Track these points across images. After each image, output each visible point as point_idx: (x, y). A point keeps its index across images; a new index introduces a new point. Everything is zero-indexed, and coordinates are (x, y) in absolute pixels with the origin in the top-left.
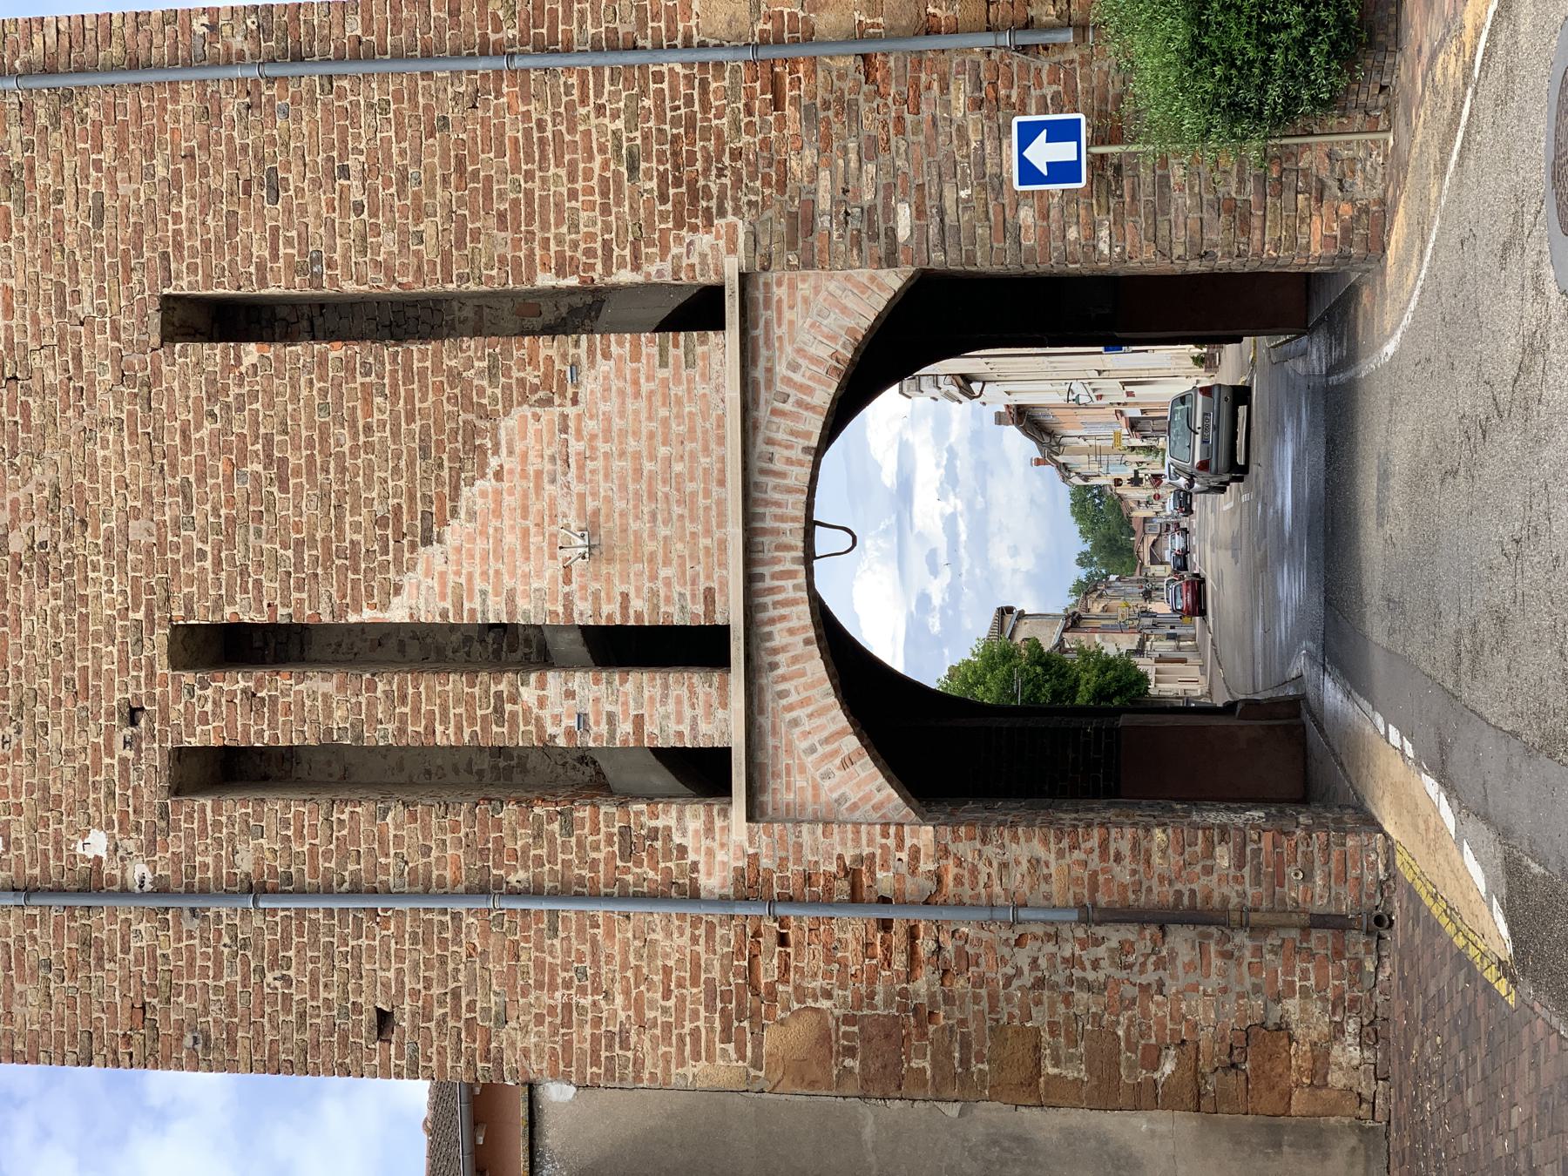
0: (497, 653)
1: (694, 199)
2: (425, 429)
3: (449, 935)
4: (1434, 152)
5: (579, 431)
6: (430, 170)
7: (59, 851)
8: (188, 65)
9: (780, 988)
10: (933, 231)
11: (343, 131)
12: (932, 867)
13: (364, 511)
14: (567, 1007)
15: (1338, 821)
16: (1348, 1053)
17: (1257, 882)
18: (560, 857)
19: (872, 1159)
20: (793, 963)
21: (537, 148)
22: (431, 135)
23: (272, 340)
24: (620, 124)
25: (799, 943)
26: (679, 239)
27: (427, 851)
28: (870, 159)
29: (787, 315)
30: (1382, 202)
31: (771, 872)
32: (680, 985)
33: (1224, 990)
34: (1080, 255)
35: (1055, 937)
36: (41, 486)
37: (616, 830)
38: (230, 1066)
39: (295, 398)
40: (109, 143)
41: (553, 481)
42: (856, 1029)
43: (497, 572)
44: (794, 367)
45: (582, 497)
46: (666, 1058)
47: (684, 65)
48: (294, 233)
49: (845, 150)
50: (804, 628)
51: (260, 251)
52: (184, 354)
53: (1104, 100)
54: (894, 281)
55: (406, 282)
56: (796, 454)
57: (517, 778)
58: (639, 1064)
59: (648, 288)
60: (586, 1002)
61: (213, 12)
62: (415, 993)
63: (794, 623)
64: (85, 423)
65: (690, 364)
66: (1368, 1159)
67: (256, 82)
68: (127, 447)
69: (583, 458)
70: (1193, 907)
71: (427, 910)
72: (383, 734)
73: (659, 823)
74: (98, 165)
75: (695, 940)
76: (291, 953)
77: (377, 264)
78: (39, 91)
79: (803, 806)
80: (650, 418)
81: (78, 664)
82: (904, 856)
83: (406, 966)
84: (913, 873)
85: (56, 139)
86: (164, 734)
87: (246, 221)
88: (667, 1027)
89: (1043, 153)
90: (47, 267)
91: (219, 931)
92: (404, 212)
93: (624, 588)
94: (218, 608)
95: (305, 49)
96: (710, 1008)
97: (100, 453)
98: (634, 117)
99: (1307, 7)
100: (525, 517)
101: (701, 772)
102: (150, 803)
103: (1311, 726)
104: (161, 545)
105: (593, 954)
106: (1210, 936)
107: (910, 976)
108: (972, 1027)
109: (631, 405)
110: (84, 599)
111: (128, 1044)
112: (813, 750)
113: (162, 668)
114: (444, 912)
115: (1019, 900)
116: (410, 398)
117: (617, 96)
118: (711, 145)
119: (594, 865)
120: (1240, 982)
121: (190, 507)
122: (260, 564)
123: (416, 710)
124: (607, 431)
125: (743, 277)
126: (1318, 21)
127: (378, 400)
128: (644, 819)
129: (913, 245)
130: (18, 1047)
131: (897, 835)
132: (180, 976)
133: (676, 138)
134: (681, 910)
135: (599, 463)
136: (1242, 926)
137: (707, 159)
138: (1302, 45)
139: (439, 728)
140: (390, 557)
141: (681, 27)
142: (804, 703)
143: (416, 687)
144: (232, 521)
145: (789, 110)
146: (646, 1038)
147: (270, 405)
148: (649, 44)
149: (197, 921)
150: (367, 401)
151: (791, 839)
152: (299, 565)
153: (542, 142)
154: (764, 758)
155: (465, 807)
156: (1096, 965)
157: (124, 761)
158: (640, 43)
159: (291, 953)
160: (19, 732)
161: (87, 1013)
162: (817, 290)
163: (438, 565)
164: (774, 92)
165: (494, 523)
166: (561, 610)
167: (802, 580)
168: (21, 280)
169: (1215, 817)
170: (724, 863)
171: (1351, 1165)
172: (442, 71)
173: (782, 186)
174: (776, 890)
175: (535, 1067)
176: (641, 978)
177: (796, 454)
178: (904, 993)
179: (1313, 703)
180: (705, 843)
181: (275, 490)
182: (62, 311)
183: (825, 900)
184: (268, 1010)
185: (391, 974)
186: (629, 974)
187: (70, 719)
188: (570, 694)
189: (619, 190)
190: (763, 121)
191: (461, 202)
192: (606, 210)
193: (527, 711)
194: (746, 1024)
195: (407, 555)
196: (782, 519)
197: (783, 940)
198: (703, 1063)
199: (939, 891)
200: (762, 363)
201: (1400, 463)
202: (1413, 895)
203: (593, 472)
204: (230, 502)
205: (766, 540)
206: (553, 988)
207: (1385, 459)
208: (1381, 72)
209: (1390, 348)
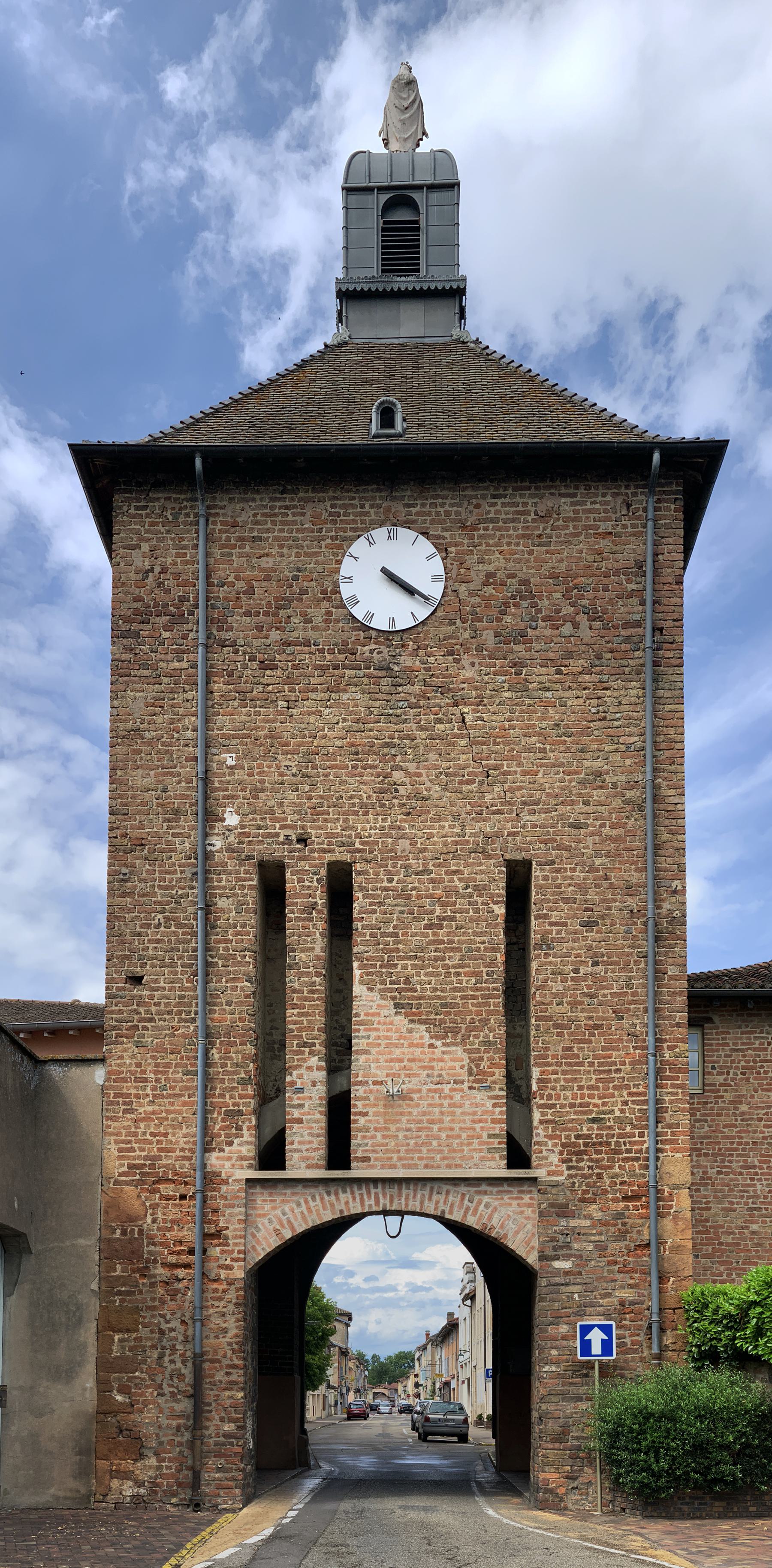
0: (335, 1044)
1: (577, 1153)
2: (457, 1005)
3: (184, 1016)
4: (592, 1535)
5: (455, 1090)
6: (595, 1010)
8: (655, 877)
9: (157, 1196)
10: (557, 1280)
11: (617, 963)
12: (222, 1277)
13: (414, 971)
14: (145, 1080)
15: (248, 1485)
16: (129, 1490)
17: (217, 1444)
19: (68, 1243)
20: (171, 1202)
21: (606, 1069)
22: (614, 1012)
23: (507, 921)
24: (617, 1114)
25: (181, 1206)
26: (555, 1145)
27: (229, 1004)
28: (595, 1247)
29: (515, 1203)
30: (566, 1509)
31: (219, 1191)
32: (158, 1142)
33: (160, 1427)
34: (543, 1356)
35: (186, 1341)
36: (428, 790)
38: (111, 893)
39: (475, 934)
40: (614, 832)
41: (428, 1076)
43: (380, 1045)
44: (487, 1206)
45: (420, 1091)
46: (119, 1134)
47: (647, 1149)
48: (564, 935)
49: (600, 1234)
50: (349, 1210)
51: (555, 916)
52: (500, 872)
53: (622, 1369)
54: (532, 1259)
55: (536, 997)
56: (441, 1206)
57: (269, 1054)
58: (116, 1119)
59: (530, 1128)
60: (148, 1091)
61: (683, 892)
63: (351, 1205)
64: (464, 816)
66: (74, 1499)
67: (645, 915)
68: (450, 839)
69: (440, 1092)
70: (203, 1412)
71: (197, 1004)
72: (293, 981)
73: (245, 1132)
74: (603, 826)
75: (182, 1150)
76: (173, 929)
77: (546, 981)
78: (644, 793)
79: (255, 1208)
80: (461, 1128)
81: (331, 810)
82: (228, 1262)
83: (167, 992)
84: (219, 1267)
86: (289, 858)
88: (135, 1135)
89: (596, 1337)
90: (549, 795)
91: (184, 888)
92: (574, 996)
93: (371, 1113)
94: (362, 889)
95: (662, 943)
96: (146, 1158)
97: (446, 824)
98: (620, 1121)
99: (667, 1472)
100: (409, 1060)
101: (272, 1154)
102: (254, 850)
103: (295, 1472)
104: (396, 858)
105: (174, 1095)
106: (188, 1420)
107: (164, 1265)
108: (139, 1297)
109: (467, 1118)
110: (366, 813)
111: (122, 836)
112: (284, 1214)
113: (328, 857)
114: (196, 1013)
115: (205, 1322)
116: (474, 997)
117: (633, 1111)
118: (605, 1163)
120: (165, 1435)
121: (417, 874)
122: (385, 913)
123: (306, 999)
124: (454, 1105)
125: (535, 1179)
126: (659, 1477)
127: (473, 980)
128: (247, 1123)
129: (550, 1269)
130: (119, 773)
132: (160, 866)
133: (609, 1144)
134: (198, 1143)
135: (437, 1101)
136: (194, 1436)
137: (598, 1161)
138: (648, 1469)
139: (295, 1011)
140: (388, 986)
141: (668, 1147)
142: (309, 1209)
143: (318, 999)
144: (409, 897)
145: (622, 1204)
146: (129, 1123)
147: (472, 920)
148: (659, 1130)
150: (473, 974)
151: (236, 1202)
152: (384, 935)
154: (280, 1189)
155: (253, 1025)
156: (172, 1361)
157: (277, 835)
158: (660, 1125)
159: (173, 929)
160: (293, 775)
161: (139, 813)
162: (527, 1218)
164: (632, 1196)
165: (406, 1043)
166: (359, 1079)
167: (374, 1209)
168: (541, 781)
169: (249, 1423)
170: (223, 1166)
171: (71, 1490)
172: (648, 1018)
174: (209, 1194)
175: (113, 1062)
176: (161, 1120)
177: (441, 1206)
178: (155, 1261)
179: (307, 1474)
180: (235, 1156)
181: (426, 922)
182: (525, 803)
183: (204, 1221)
184: (142, 915)
185: (162, 984)
186: (164, 1114)
187: (300, 805)
188: (314, 1084)
190: (617, 1191)
194: (138, 1177)
196: (407, 1199)
197: (183, 1197)
198: (117, 1154)
199: (210, 1280)
200: (489, 1189)
201: (432, 1518)
202: (211, 1522)
203: (433, 1097)
205: (396, 1190)
206: (156, 1072)
207: (433, 1510)
208: (632, 1509)
209: (491, 1512)
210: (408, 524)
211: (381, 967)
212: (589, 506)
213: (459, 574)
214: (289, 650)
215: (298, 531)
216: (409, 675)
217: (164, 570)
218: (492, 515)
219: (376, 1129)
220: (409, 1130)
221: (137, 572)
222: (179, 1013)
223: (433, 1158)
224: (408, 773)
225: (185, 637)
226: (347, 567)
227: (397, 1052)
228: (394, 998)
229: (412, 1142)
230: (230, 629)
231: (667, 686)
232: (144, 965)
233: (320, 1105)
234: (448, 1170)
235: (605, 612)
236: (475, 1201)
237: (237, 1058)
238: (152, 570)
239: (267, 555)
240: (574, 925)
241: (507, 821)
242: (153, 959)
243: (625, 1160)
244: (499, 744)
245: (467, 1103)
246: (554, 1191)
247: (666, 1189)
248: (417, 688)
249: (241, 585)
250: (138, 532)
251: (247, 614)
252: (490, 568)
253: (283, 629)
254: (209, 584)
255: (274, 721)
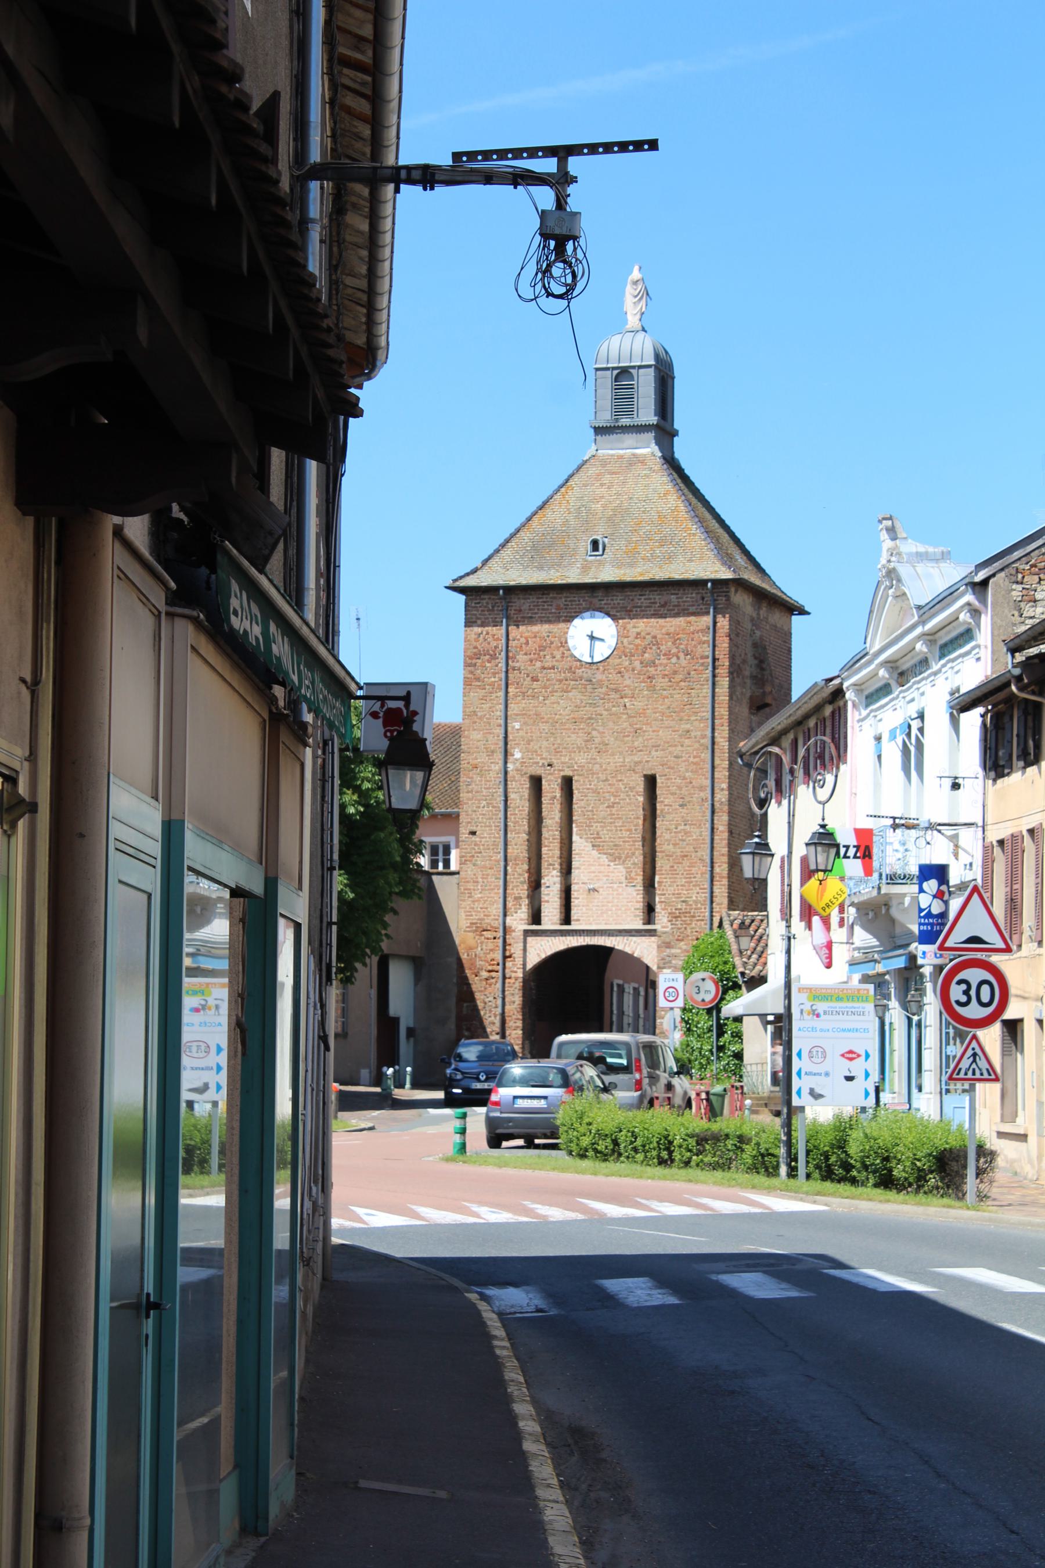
51: (667, 801)
65: (636, 916)
72: (545, 834)
98: (696, 902)
101: (536, 917)
113: (562, 774)
125: (655, 930)
176: (485, 901)
183: (504, 950)
210: (600, 610)
216: (600, 684)
224: (599, 732)
227: (593, 868)
237: (519, 871)
248: (604, 689)
249: (523, 640)
251: (526, 654)
252: (638, 630)
254: (508, 639)
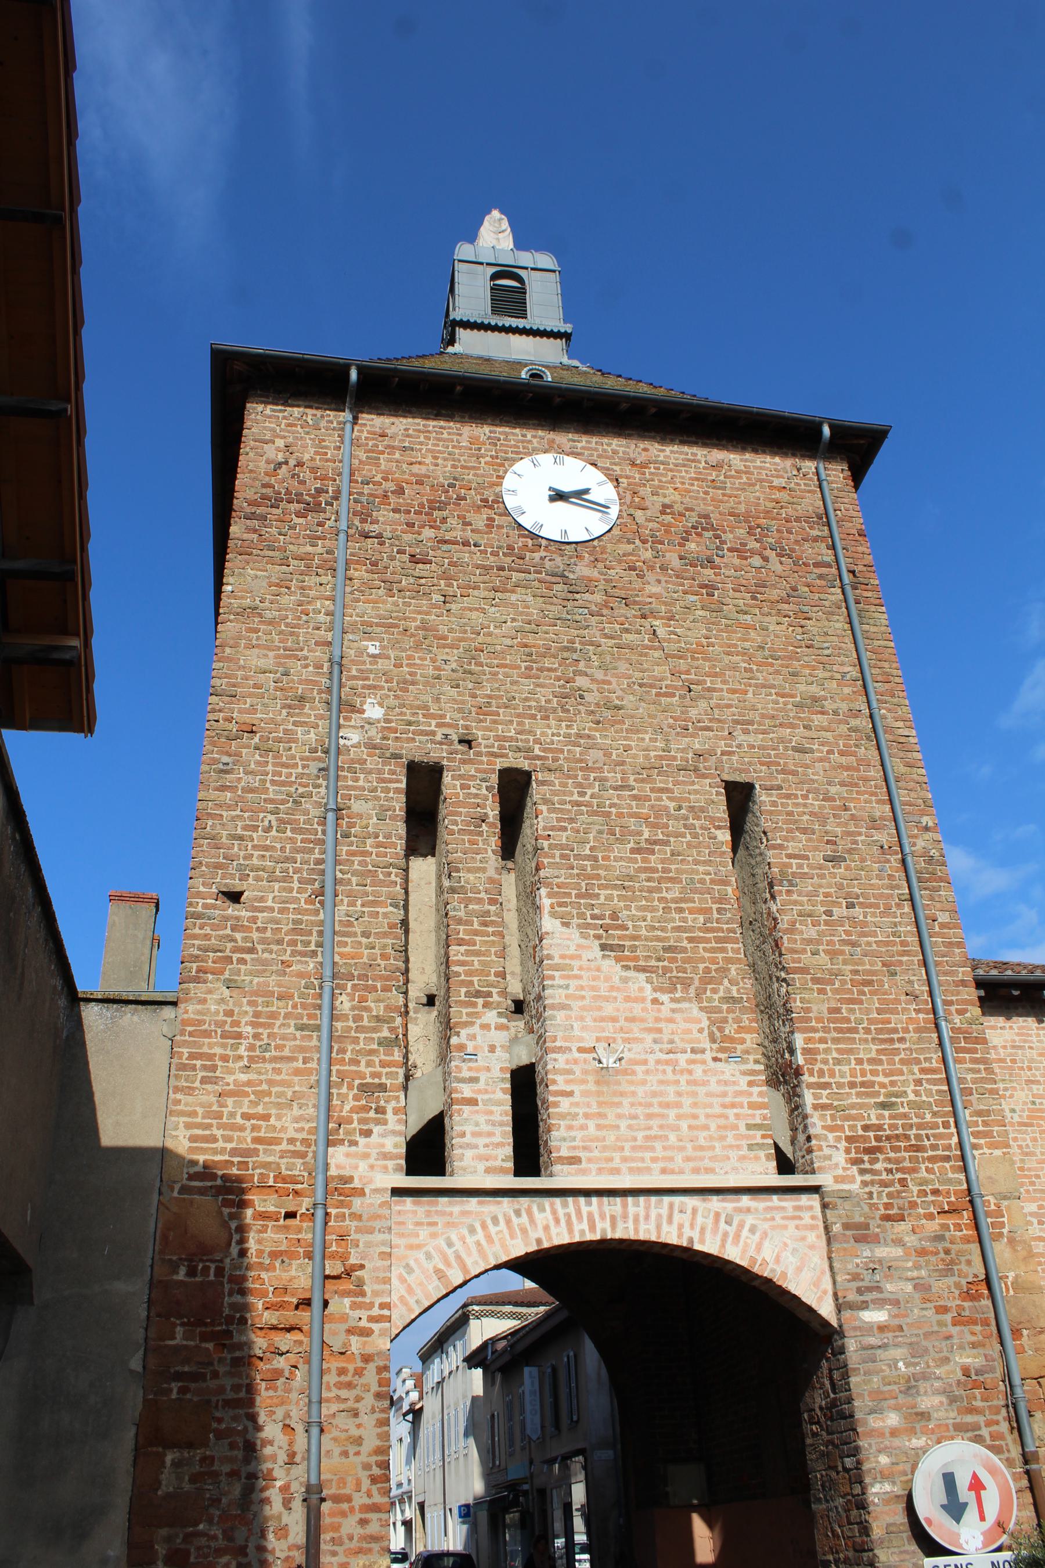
1: (869, 1151)
2: (684, 950)
3: (299, 947)
6: (863, 964)
7: (369, 687)
10: (872, 1341)
13: (622, 904)
14: (239, 1036)
18: (362, 1036)
21: (887, 1037)
22: (884, 965)
24: (912, 1097)
26: (838, 1139)
27: (366, 934)
28: (915, 1287)
31: (349, 1206)
32: (254, 1128)
37: (384, 1080)
39: (696, 862)
40: (843, 760)
41: (655, 1041)
42: (212, 1277)
43: (583, 998)
44: (753, 1230)
45: (645, 1062)
46: (194, 1114)
48: (806, 870)
49: (917, 1267)
50: (550, 1239)
51: (792, 847)
52: (718, 794)
54: (826, 1310)
58: (189, 1091)
62: (254, 919)
63: (554, 1230)
68: (652, 754)
73: (390, 1115)
75: (291, 1141)
76: (289, 834)
77: (794, 923)
80: (707, 1116)
81: (501, 711)
82: (364, 1323)
83: (275, 914)
84: (350, 1331)
85: (843, 728)
86: (453, 760)
87: (809, 840)
88: (219, 1116)
90: (763, 716)
93: (577, 1093)
94: (546, 801)
96: (234, 1152)
97: (647, 737)
100: (627, 1019)
102: (402, 748)
104: (587, 769)
105: (282, 1058)
109: (716, 1101)
110: (547, 718)
111: (226, 720)
112: (450, 1244)
113: (500, 764)
116: (707, 941)
118: (907, 1164)
119: (357, 1062)
121: (616, 789)
122: (578, 831)
123: (476, 933)
124: (695, 1083)
125: (815, 1189)
127: (701, 918)
128: (393, 1104)
131: (382, 1316)
132: (274, 757)
135: (670, 1076)
137: (897, 1161)
139: (462, 949)
141: (982, 1141)
142: (489, 1238)
149: (315, 772)
153: (891, 1041)
157: (433, 733)
159: (289, 834)
162: (812, 1247)
163: (586, 955)
166: (558, 1044)
170: (356, 1167)
173: (887, 1218)
177: (687, 1232)
180: (374, 1152)
181: (632, 845)
184: (246, 815)
185: (269, 903)
186: (265, 1087)
187: (463, 702)
188: (492, 1049)
189: (868, 1095)
191: (843, 982)
192: (852, 1085)
193: (477, 1015)
195: (592, 932)
197: (290, 1215)
203: (664, 1072)
204: (620, 815)
206: (254, 1025)
211: (578, 896)
212: (758, 464)
213: (632, 502)
214: (445, 547)
215: (454, 447)
216: (589, 585)
217: (300, 464)
218: (661, 458)
219: (587, 1116)
220: (635, 1117)
221: (268, 462)
222: (293, 943)
223: (671, 1159)
224: (594, 681)
225: (321, 524)
226: (509, 481)
228: (598, 937)
229: (640, 1135)
230: (377, 522)
231: (871, 621)
232: (244, 877)
233: (503, 1080)
234: (694, 1177)
235: (792, 550)
236: (735, 1223)
237: (378, 1009)
238: (286, 463)
239: (420, 463)
240: (818, 858)
241: (716, 737)
242: (258, 870)
243: (932, 1159)
244: (698, 659)
245: (713, 1080)
246: (847, 1205)
247: (992, 1200)
248: (598, 597)
249: (391, 486)
250: (273, 430)
251: (395, 511)
252: (667, 501)
253: (438, 528)
255: (427, 613)
